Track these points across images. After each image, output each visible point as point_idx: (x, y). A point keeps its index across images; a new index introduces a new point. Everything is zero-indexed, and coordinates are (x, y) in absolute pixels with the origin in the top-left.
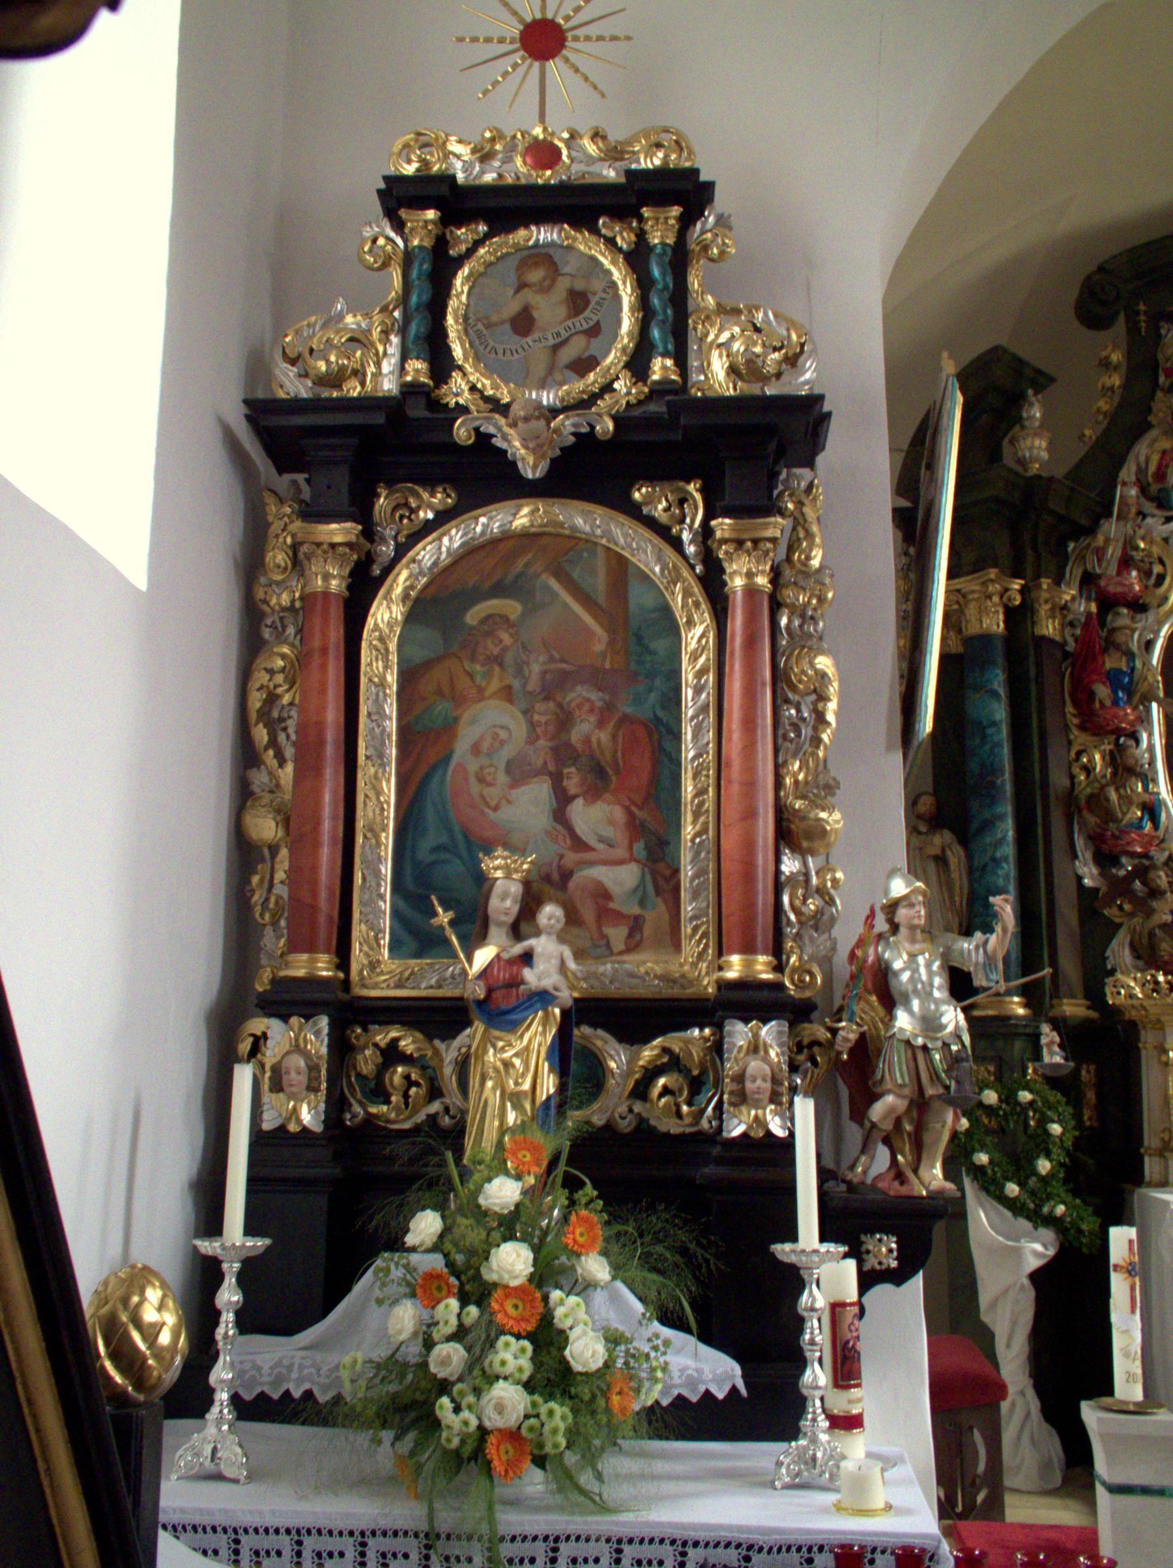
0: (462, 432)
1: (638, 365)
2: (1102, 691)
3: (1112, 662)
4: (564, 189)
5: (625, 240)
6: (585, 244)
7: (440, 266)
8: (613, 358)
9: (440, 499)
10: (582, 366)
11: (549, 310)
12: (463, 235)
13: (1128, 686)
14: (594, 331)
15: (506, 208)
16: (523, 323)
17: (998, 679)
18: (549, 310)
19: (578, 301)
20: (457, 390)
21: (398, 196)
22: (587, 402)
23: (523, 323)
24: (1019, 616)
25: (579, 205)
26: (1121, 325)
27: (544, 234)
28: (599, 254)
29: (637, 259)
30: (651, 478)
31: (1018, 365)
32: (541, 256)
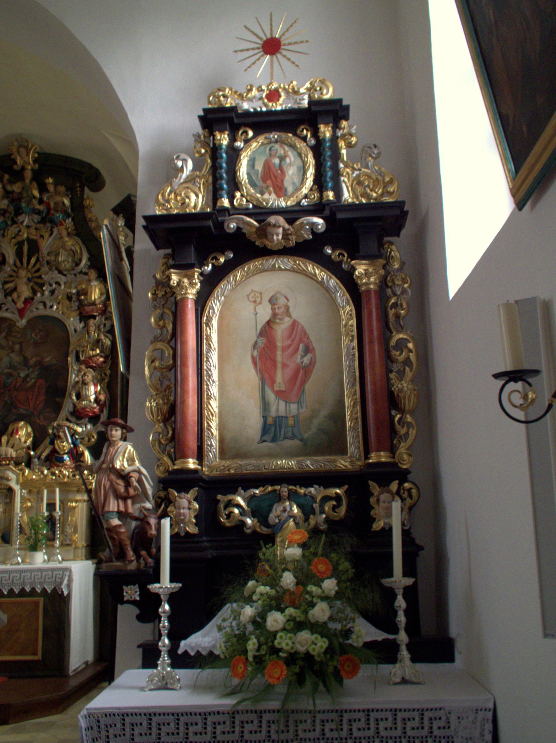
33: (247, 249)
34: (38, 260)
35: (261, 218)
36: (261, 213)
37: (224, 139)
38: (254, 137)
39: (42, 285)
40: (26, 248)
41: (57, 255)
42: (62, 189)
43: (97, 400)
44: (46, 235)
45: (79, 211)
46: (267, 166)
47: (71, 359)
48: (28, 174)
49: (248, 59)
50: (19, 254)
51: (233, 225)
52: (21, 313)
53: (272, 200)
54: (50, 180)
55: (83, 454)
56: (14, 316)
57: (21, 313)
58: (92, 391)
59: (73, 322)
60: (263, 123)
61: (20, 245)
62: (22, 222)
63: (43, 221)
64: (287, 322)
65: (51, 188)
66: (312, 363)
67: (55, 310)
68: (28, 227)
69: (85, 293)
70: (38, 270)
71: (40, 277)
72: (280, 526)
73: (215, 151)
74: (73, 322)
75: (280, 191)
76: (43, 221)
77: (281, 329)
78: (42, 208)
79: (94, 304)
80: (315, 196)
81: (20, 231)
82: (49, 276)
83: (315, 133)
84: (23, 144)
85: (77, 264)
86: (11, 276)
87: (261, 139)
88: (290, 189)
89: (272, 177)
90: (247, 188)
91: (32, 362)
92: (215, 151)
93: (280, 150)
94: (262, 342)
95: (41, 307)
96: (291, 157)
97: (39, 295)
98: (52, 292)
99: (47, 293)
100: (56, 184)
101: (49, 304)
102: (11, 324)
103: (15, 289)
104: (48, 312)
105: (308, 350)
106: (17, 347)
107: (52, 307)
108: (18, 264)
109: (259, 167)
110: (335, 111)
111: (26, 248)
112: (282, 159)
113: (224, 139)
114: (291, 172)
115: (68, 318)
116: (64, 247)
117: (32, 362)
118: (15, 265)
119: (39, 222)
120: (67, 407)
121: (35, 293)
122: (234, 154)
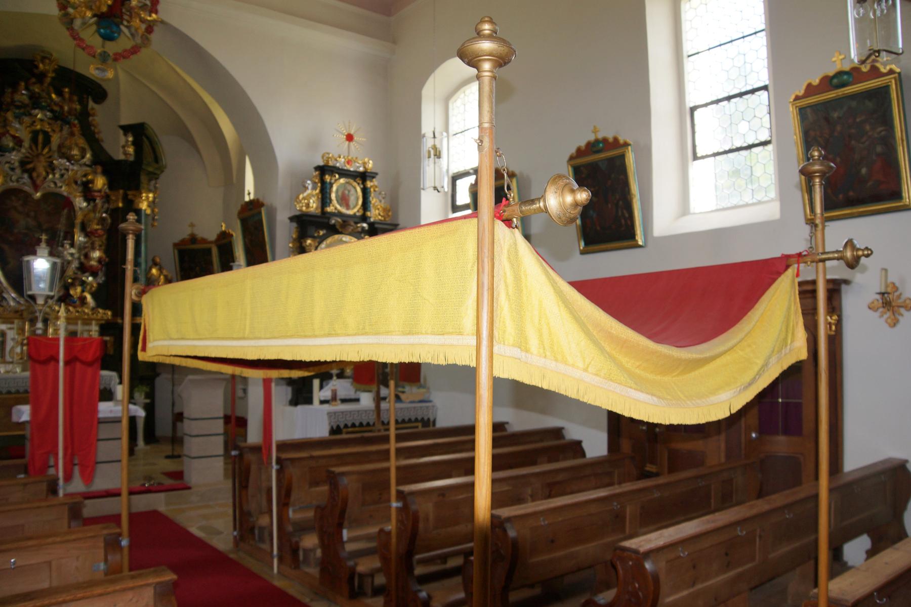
33: (334, 230)
34: (50, 150)
35: (345, 219)
36: (340, 214)
37: (328, 178)
38: (340, 178)
40: (41, 138)
41: (71, 149)
42: (75, 98)
44: (57, 130)
45: (84, 116)
46: (343, 194)
48: (48, 80)
49: (435, 227)
50: (34, 140)
51: (333, 222)
53: (344, 210)
54: (67, 90)
55: (85, 298)
58: (97, 254)
59: (80, 203)
60: (344, 173)
61: (35, 135)
62: (36, 116)
65: (67, 96)
67: (64, 190)
68: (41, 120)
69: (92, 182)
70: (50, 157)
71: (52, 162)
73: (323, 182)
74: (80, 203)
75: (348, 207)
78: (56, 108)
79: (100, 191)
81: (34, 122)
82: (58, 162)
84: (46, 57)
85: (83, 157)
86: (27, 157)
87: (342, 181)
88: (352, 206)
89: (344, 200)
90: (335, 202)
91: (44, 227)
92: (323, 182)
93: (349, 187)
95: (52, 185)
97: (51, 176)
98: (62, 176)
99: (57, 176)
100: (71, 93)
101: (59, 184)
102: (28, 196)
103: (34, 169)
104: (58, 190)
106: (32, 214)
107: (61, 187)
108: (34, 148)
109: (340, 193)
110: (373, 176)
111: (41, 138)
112: (349, 191)
113: (328, 178)
115: (75, 197)
116: (77, 145)
117: (44, 227)
118: (31, 148)
119: (50, 119)
121: (48, 174)
122: (331, 185)
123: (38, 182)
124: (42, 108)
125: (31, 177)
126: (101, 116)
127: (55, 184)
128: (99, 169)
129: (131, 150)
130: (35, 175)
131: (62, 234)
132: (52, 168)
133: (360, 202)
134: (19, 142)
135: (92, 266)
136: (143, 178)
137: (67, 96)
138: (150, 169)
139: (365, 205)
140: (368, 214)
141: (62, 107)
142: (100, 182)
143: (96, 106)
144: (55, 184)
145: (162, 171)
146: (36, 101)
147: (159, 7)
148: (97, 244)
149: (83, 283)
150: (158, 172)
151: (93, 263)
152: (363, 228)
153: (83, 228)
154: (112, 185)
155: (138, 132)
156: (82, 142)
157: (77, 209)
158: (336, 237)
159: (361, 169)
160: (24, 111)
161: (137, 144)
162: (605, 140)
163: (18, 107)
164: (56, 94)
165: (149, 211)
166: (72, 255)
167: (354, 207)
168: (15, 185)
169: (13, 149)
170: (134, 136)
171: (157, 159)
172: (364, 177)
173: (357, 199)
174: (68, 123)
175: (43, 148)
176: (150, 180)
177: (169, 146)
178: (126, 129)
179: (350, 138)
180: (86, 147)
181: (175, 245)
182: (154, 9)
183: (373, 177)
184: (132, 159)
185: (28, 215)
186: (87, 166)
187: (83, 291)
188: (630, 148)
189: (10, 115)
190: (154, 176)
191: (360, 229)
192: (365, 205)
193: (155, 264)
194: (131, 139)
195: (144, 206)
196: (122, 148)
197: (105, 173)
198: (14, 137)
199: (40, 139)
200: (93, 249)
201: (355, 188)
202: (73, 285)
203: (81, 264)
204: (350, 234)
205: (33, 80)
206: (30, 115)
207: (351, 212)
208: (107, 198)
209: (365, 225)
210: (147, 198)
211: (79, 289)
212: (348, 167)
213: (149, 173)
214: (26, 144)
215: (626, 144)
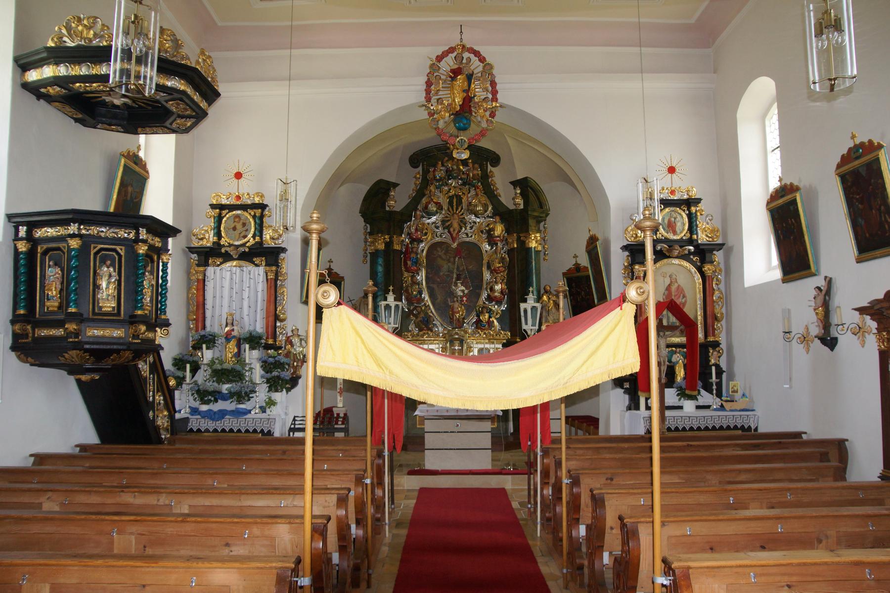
0: (223, 250)
1: (254, 237)
2: (409, 263)
3: (413, 255)
4: (241, 205)
5: (253, 213)
6: (246, 214)
7: (219, 219)
8: (250, 236)
9: (221, 260)
10: (245, 237)
11: (239, 226)
12: (224, 212)
13: (417, 262)
14: (247, 230)
15: (231, 208)
16: (234, 229)
17: (380, 261)
18: (239, 226)
19: (244, 225)
20: (223, 242)
21: (213, 206)
22: (244, 245)
23: (234, 229)
24: (388, 245)
25: (244, 207)
26: (420, 169)
27: (239, 212)
28: (247, 216)
29: (254, 217)
30: (256, 257)
31: (388, 183)
32: (238, 216)
35: (670, 244)
39: (465, 224)
42: (476, 166)
43: (502, 292)
45: (485, 178)
46: (669, 221)
47: (484, 269)
50: (451, 203)
52: (453, 239)
53: (671, 236)
56: (450, 241)
57: (453, 239)
58: (498, 287)
59: (486, 247)
61: (451, 198)
63: (464, 184)
64: (676, 285)
66: (686, 302)
68: (454, 187)
69: (493, 230)
72: (678, 362)
75: (675, 233)
76: (464, 184)
77: (674, 288)
80: (689, 235)
83: (689, 209)
85: (486, 211)
94: (666, 293)
96: (679, 217)
98: (471, 228)
105: (684, 296)
110: (698, 201)
112: (675, 218)
114: (679, 225)
120: (484, 295)
121: (461, 228)
123: (454, 235)
124: (454, 178)
125: (449, 232)
126: (500, 178)
127: (467, 234)
128: (498, 218)
129: (520, 201)
130: (452, 230)
131: (455, 276)
132: (463, 223)
133: (686, 227)
134: (440, 207)
135: (496, 297)
136: (532, 222)
137: (471, 165)
138: (536, 214)
139: (692, 229)
140: (695, 237)
141: (468, 175)
142: (499, 230)
143: (493, 169)
144: (467, 234)
145: (547, 215)
146: (449, 174)
147: (498, 96)
148: (499, 280)
149: (490, 311)
150: (544, 215)
151: (496, 294)
152: (689, 250)
153: (489, 267)
154: (508, 230)
155: (525, 186)
156: (484, 199)
157: (484, 252)
158: (665, 260)
159: (686, 197)
160: (443, 182)
161: (524, 195)
162: (862, 145)
163: (438, 181)
164: (463, 165)
165: (540, 248)
166: (463, 291)
167: (681, 232)
168: (437, 239)
169: (437, 213)
170: (521, 188)
171: (541, 205)
172: (689, 203)
173: (684, 225)
174: (474, 186)
175: (457, 209)
176: (539, 222)
177: (552, 191)
178: (515, 184)
179: (672, 170)
180: (489, 203)
181: (564, 274)
182: (495, 99)
183: (699, 203)
184: (522, 207)
185: (449, 261)
186: (491, 217)
187: (490, 317)
188: (882, 150)
189: (432, 188)
190: (539, 220)
191: (687, 252)
192: (692, 229)
193: (546, 292)
194: (519, 192)
195: (533, 244)
196: (510, 199)
197: (503, 220)
198: (436, 203)
199: (455, 201)
200: (496, 283)
201: (680, 214)
202: (482, 312)
203: (489, 296)
204: (677, 257)
205: (446, 158)
206: (447, 184)
207: (675, 238)
208: (505, 241)
209: (691, 248)
210: (535, 237)
211: (487, 316)
212: (672, 197)
213: (535, 217)
214: (445, 207)
215: (880, 147)
